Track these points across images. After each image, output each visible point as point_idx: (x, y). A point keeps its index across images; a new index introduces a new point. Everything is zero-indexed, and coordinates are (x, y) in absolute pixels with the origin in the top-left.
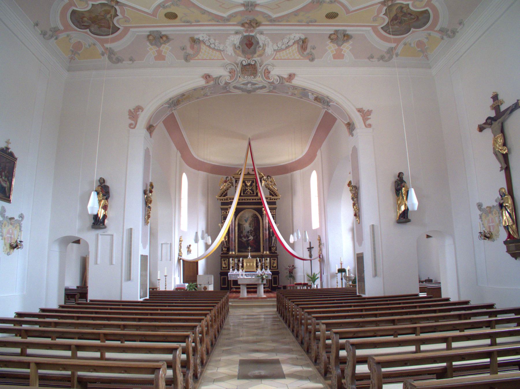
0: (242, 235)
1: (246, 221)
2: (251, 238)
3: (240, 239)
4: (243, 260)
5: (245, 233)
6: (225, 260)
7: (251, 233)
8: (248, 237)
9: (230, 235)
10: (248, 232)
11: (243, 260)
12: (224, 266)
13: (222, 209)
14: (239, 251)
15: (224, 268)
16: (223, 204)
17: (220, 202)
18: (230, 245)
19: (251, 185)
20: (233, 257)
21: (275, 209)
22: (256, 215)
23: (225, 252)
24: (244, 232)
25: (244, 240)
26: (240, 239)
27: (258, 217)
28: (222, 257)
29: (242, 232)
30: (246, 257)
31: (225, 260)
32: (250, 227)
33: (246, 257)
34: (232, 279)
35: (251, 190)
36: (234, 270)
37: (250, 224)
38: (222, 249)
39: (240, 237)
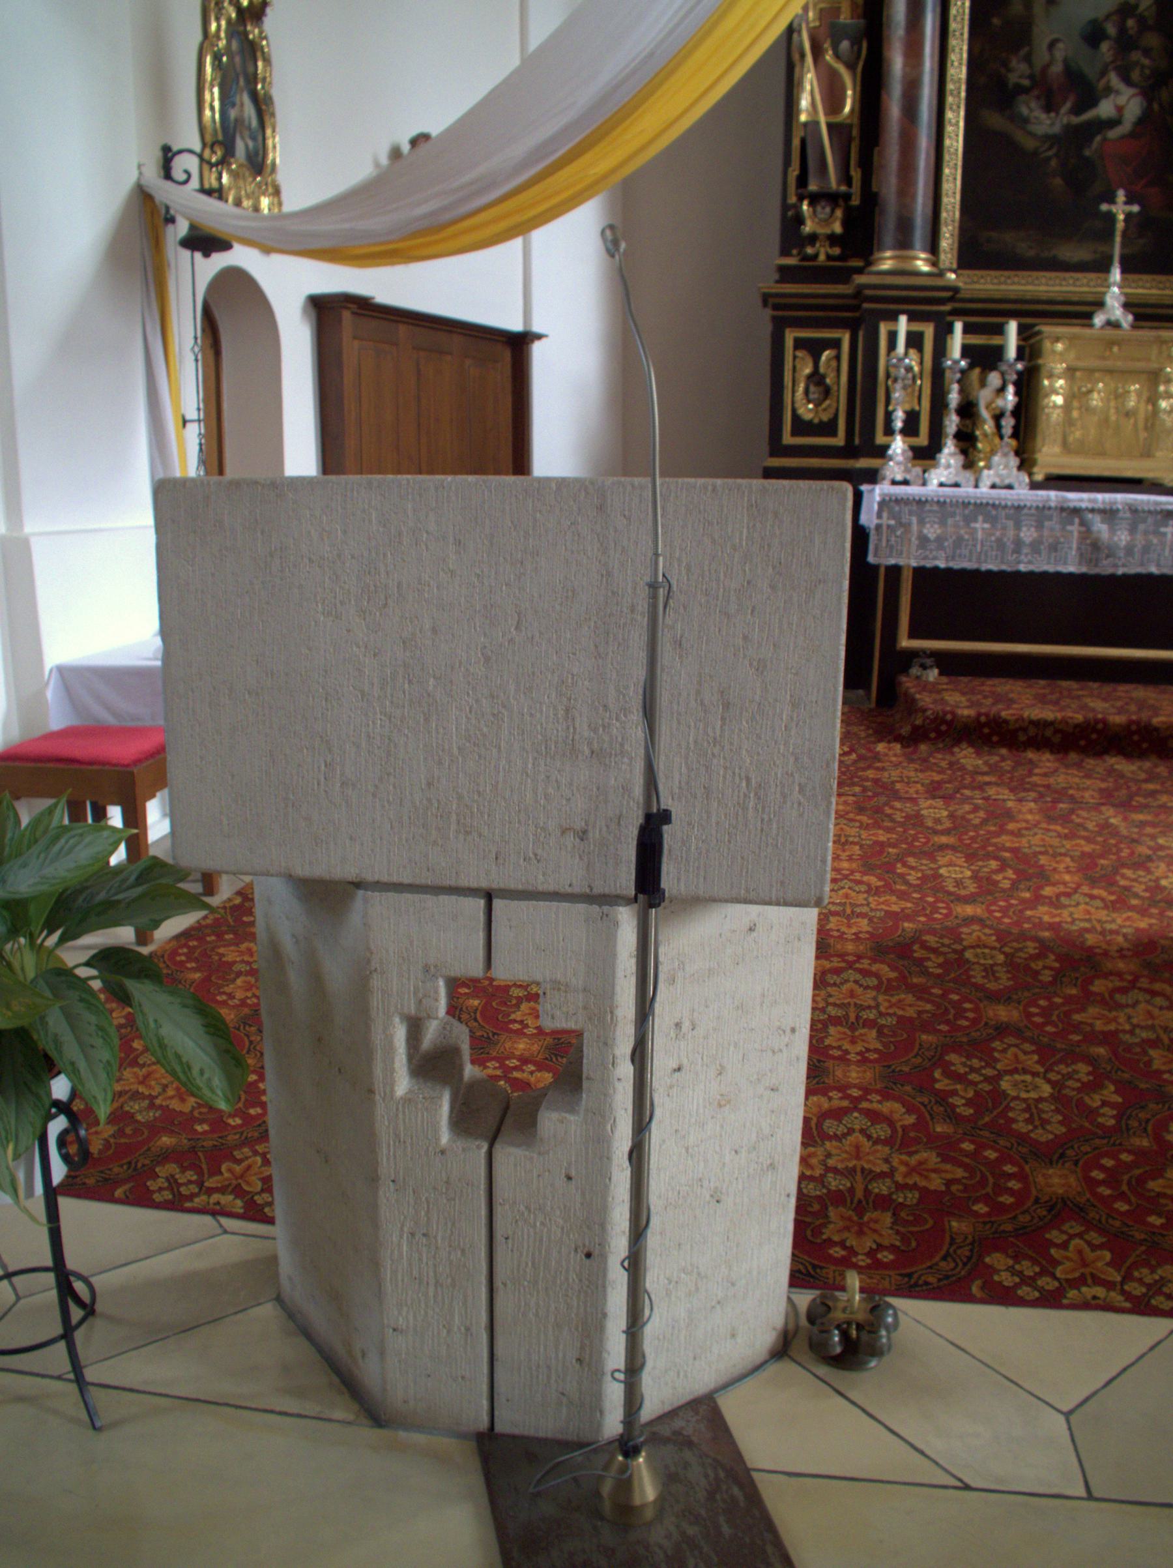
0: (1018, 72)
3: (994, 120)
4: (1029, 350)
6: (814, 348)
7: (1125, 43)
8: (1088, 96)
9: (897, 63)
10: (1093, 35)
11: (1029, 350)
12: (807, 411)
14: (972, 255)
15: (801, 427)
18: (888, 185)
20: (932, 306)
23: (822, 253)
24: (1044, 31)
25: (1042, 123)
26: (994, 120)
28: (784, 313)
30: (1080, 312)
31: (814, 348)
33: (1080, 312)
34: (910, 559)
36: (925, 455)
38: (792, 223)
39: (988, 91)
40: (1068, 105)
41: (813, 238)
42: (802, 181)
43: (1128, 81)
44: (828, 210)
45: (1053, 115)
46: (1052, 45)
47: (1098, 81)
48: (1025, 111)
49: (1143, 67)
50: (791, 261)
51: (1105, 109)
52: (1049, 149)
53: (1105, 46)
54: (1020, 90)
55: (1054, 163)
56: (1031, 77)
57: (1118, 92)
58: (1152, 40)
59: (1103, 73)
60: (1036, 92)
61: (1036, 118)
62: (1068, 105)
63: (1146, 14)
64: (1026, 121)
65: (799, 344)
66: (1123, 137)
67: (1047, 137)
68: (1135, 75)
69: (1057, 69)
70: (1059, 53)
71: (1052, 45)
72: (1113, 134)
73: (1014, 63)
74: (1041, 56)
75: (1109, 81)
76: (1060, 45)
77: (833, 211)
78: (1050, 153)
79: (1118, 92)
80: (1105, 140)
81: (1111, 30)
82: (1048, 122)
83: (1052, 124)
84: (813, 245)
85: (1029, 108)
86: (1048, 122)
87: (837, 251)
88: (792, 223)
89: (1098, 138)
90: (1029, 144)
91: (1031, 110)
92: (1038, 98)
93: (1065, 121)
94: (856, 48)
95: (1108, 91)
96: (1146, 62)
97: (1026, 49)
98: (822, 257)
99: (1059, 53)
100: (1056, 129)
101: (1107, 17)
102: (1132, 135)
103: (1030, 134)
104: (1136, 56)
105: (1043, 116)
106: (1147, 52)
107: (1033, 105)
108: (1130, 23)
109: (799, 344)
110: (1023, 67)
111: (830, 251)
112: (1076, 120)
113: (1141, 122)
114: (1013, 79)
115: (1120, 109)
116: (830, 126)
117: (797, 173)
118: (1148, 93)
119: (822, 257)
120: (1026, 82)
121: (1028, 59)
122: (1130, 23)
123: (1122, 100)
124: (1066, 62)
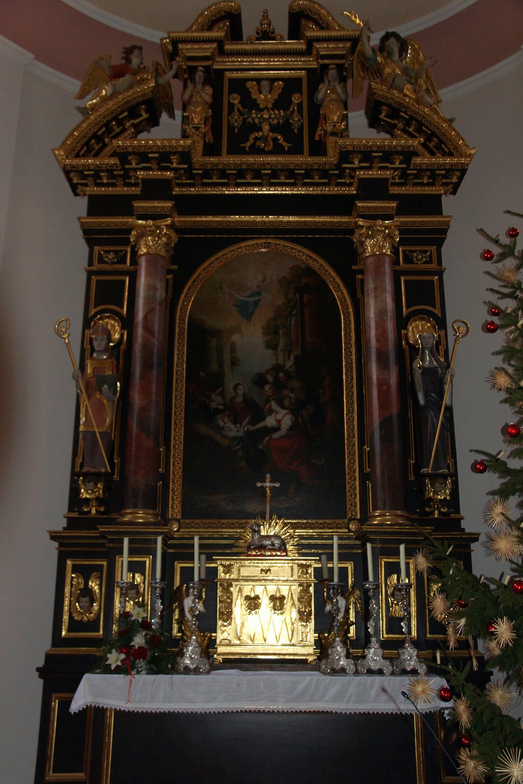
1: (246, 311)
2: (280, 419)
5: (236, 385)
7: (278, 386)
10: (260, 381)
13: (92, 236)
16: (97, 205)
17: (81, 205)
19: (283, 102)
21: (438, 236)
22: (309, 271)
24: (230, 380)
27: (321, 288)
29: (217, 382)
32: (271, 346)
35: (283, 128)
37: (272, 330)
39: (199, 412)
40: (247, 420)
41: (87, 501)
42: (82, 465)
43: (283, 407)
44: (92, 484)
45: (238, 425)
46: (236, 387)
47: (265, 406)
48: (221, 424)
49: (290, 398)
50: (75, 515)
51: (270, 421)
52: (237, 445)
53: (267, 387)
54: (217, 411)
55: (240, 453)
56: (224, 404)
57: (276, 412)
58: (295, 384)
59: (267, 401)
60: (227, 413)
61: (228, 427)
62: (247, 420)
63: (290, 370)
64: (223, 429)
65: (75, 569)
66: (281, 437)
67: (235, 438)
68: (286, 402)
69: (240, 399)
70: (241, 391)
71: (236, 387)
72: (275, 436)
73: (214, 397)
74: (230, 392)
75: (271, 406)
76: (241, 387)
77: (96, 484)
78: (238, 447)
79: (276, 412)
80: (271, 439)
81: (270, 378)
82: (236, 429)
83: (238, 431)
84: (88, 506)
85: (223, 421)
86: (236, 429)
87: (102, 509)
88: (74, 491)
89: (267, 438)
90: (225, 442)
91: (225, 423)
92: (229, 416)
93: (246, 429)
94: (112, 389)
95: (271, 411)
96: (293, 395)
97: (221, 389)
98: (94, 511)
99: (241, 391)
100: (241, 433)
101: (267, 372)
102: (287, 436)
103: (225, 436)
104: (286, 392)
105: (233, 426)
106: (292, 390)
107: (226, 420)
108: (281, 374)
109: (75, 569)
110: (219, 399)
111: (98, 509)
112: (251, 428)
113: (291, 428)
114: (213, 405)
115: (279, 421)
116: (100, 433)
117: (81, 461)
118: (295, 411)
119: (94, 511)
120: (221, 407)
121: (222, 394)
122: (281, 374)
123: (279, 417)
124: (244, 395)
